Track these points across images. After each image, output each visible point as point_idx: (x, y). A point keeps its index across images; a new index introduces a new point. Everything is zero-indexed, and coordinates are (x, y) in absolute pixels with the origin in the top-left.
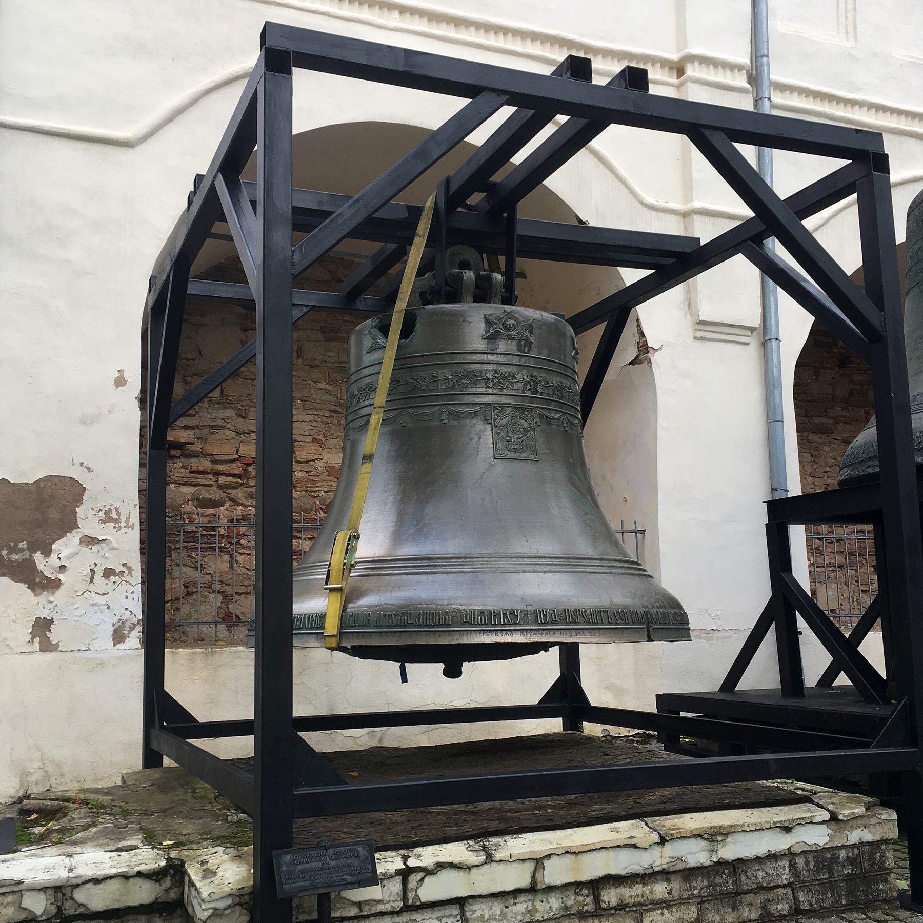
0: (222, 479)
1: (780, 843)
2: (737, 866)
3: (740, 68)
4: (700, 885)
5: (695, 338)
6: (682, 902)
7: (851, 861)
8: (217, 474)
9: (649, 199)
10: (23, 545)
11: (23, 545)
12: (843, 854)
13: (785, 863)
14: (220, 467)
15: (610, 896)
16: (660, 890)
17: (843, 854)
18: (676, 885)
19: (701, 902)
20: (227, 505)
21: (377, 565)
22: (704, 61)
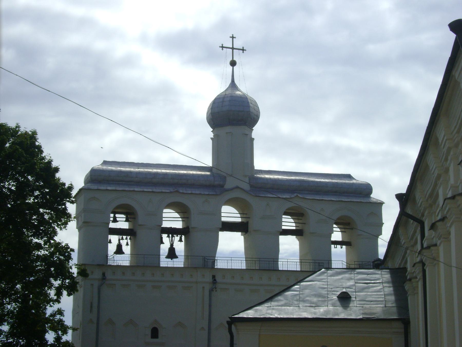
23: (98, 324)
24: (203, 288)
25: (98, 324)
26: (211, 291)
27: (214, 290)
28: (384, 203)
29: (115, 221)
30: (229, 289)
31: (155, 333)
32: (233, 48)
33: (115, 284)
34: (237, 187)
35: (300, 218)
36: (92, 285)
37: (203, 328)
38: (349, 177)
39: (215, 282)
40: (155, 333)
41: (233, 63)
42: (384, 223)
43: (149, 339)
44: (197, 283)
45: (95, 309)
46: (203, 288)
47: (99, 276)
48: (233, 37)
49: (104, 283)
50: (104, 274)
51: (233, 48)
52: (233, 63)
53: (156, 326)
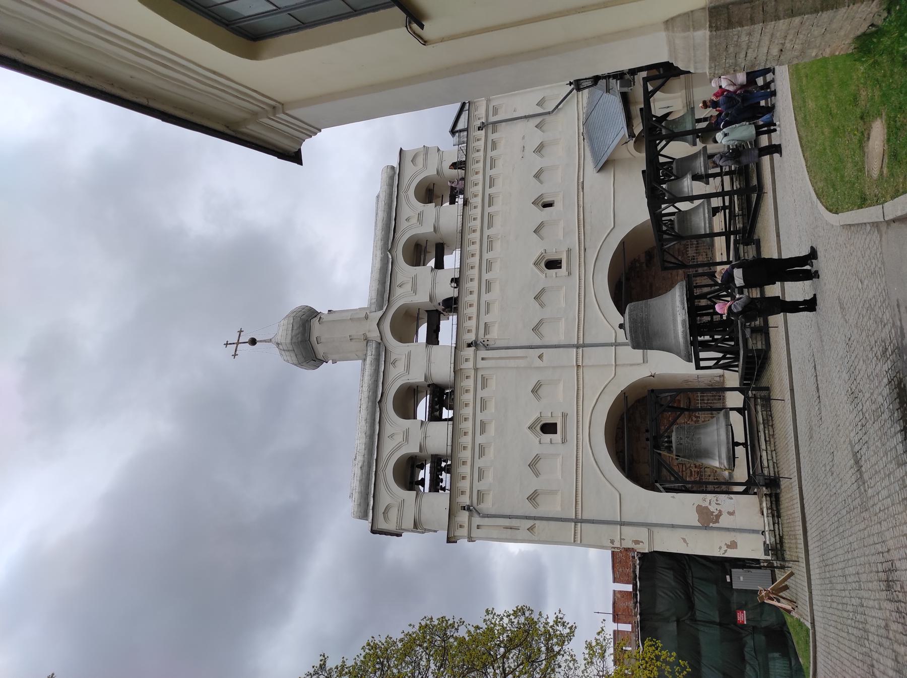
0: (684, 470)
1: (760, 413)
2: (763, 420)
3: (577, 351)
4: (766, 426)
5: (647, 362)
6: (769, 429)
7: (763, 402)
8: (683, 471)
9: (613, 375)
10: (712, 517)
11: (712, 517)
12: (762, 403)
13: (763, 412)
14: (681, 470)
15: (768, 439)
16: (767, 432)
17: (762, 403)
18: (766, 429)
19: (769, 426)
20: (691, 468)
21: (720, 463)
22: (577, 361)
23: (535, 518)
24: (483, 359)
25: (535, 518)
26: (487, 347)
27: (486, 343)
28: (401, 149)
29: (422, 482)
30: (486, 323)
31: (549, 428)
32: (238, 343)
33: (478, 491)
34: (378, 325)
35: (423, 248)
36: (478, 527)
37: (540, 357)
38: (378, 197)
39: (473, 342)
40: (549, 428)
41: (253, 342)
42: (424, 146)
43: (557, 437)
44: (476, 370)
45: (514, 523)
46: (483, 359)
47: (466, 513)
48: (227, 344)
49: (475, 510)
50: (464, 508)
51: (238, 343)
52: (253, 342)
53: (538, 428)
